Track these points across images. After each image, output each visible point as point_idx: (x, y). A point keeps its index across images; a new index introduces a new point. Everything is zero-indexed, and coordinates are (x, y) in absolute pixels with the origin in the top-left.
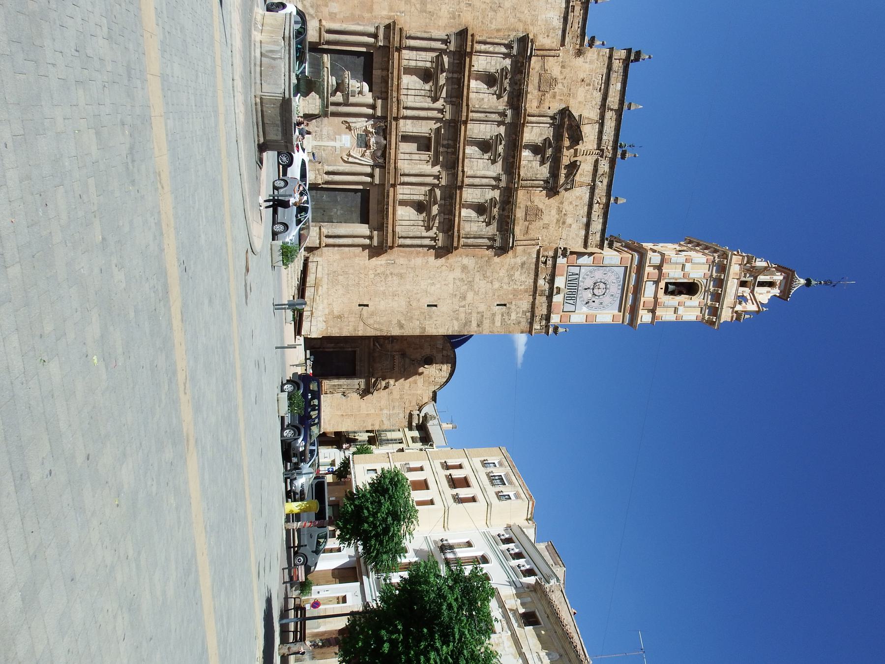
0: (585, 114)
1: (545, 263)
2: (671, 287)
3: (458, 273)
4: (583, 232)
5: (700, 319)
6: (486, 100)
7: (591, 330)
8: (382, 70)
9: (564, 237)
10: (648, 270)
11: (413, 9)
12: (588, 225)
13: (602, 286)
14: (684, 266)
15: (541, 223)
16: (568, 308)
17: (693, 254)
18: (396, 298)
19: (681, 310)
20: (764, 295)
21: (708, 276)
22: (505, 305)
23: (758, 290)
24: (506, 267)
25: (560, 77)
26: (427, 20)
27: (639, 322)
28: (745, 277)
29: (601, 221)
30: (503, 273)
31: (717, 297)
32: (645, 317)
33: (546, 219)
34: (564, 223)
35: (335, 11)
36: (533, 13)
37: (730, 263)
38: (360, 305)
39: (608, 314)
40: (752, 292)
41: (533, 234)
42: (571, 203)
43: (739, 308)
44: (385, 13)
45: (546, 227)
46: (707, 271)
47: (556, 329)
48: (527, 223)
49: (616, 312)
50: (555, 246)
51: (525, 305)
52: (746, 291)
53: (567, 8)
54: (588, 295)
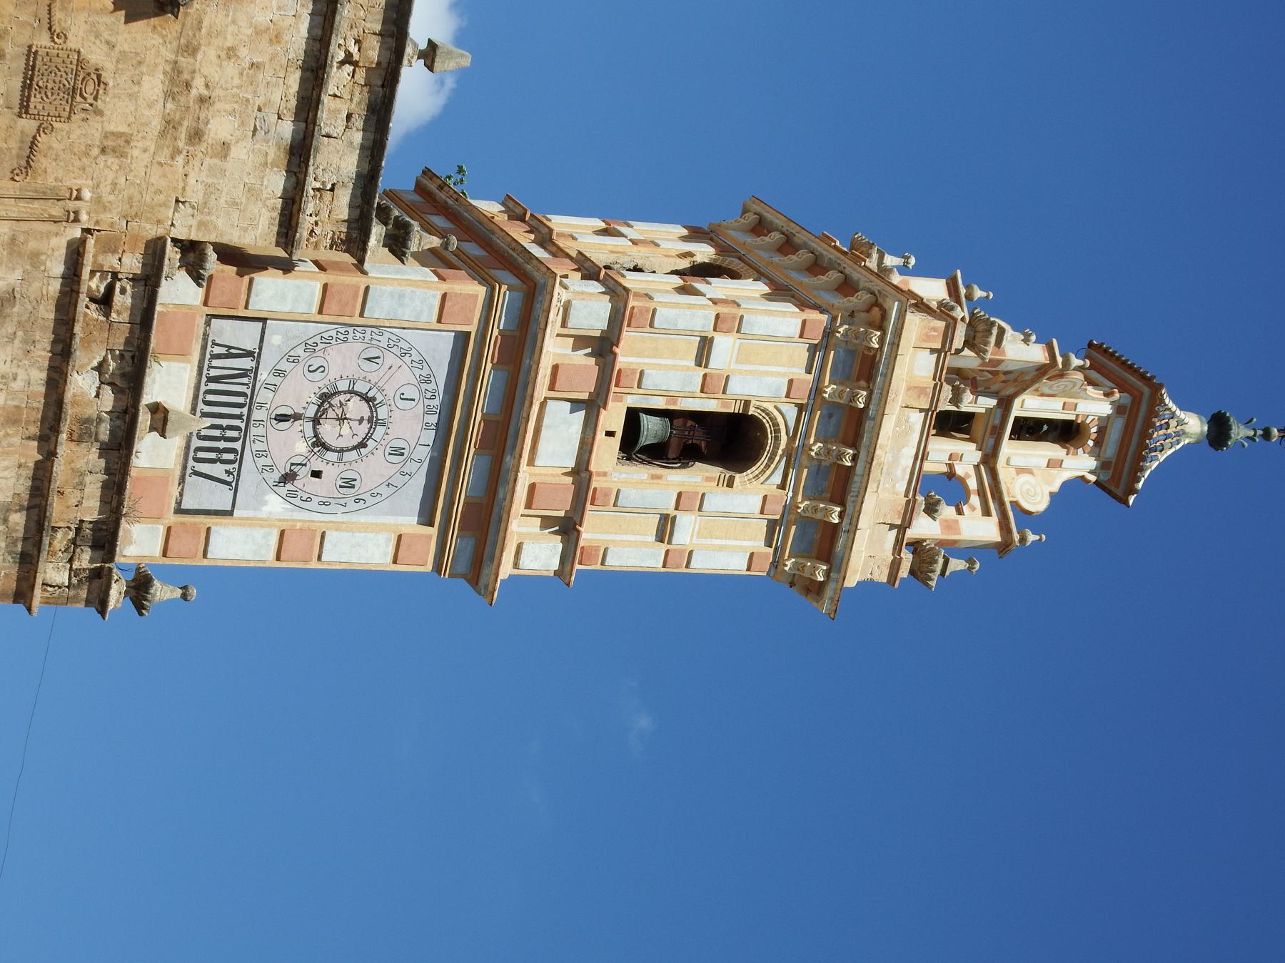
1: (105, 302)
2: (652, 429)
4: (277, 182)
5: (761, 569)
7: (298, 595)
9: (195, 194)
10: (555, 349)
12: (299, 154)
13: (356, 408)
14: (705, 346)
15: (95, 130)
16: (202, 494)
17: (749, 289)
19: (687, 530)
20: (1035, 475)
21: (802, 396)
23: (1013, 452)
27: (506, 570)
28: (956, 400)
29: (358, 137)
31: (841, 485)
32: (530, 549)
33: (117, 112)
34: (196, 135)
37: (895, 345)
39: (375, 533)
40: (989, 460)
41: (51, 172)
42: (231, 53)
43: (924, 527)
45: (115, 146)
46: (799, 372)
47: (140, 587)
48: (28, 125)
49: (409, 522)
50: (152, 231)
52: (963, 455)
54: (291, 444)
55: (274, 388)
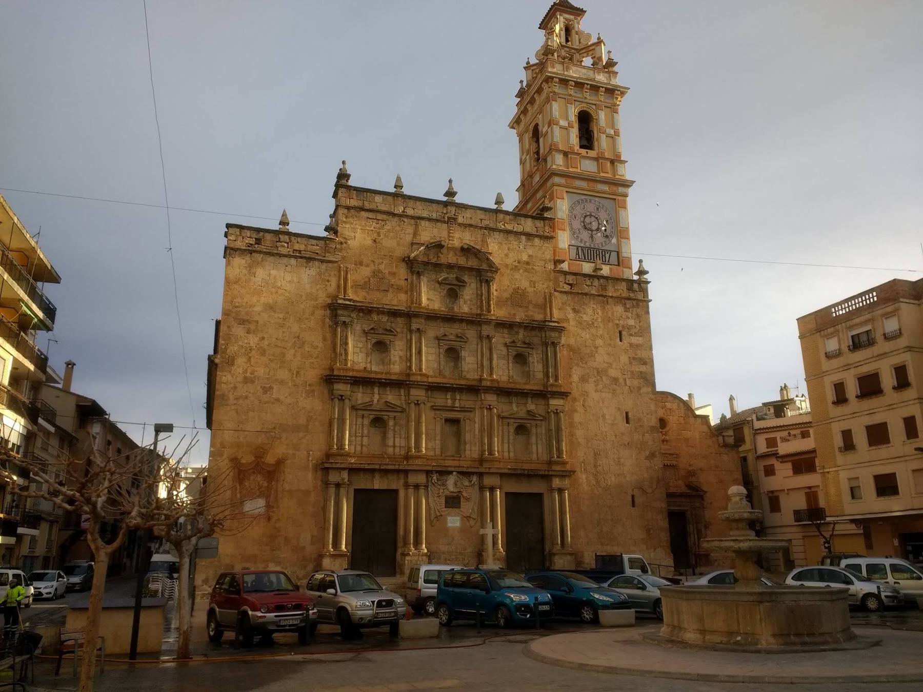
0: (409, 238)
3: (590, 387)
6: (401, 353)
8: (374, 477)
11: (304, 441)
13: (588, 220)
18: (622, 461)
22: (620, 333)
24: (579, 331)
25: (372, 267)
26: (317, 423)
30: (586, 335)
33: (525, 284)
34: (528, 263)
35: (308, 536)
36: (304, 298)
38: (633, 506)
44: (310, 476)
45: (533, 284)
48: (531, 307)
51: (619, 309)
53: (295, 257)
55: (585, 242)
